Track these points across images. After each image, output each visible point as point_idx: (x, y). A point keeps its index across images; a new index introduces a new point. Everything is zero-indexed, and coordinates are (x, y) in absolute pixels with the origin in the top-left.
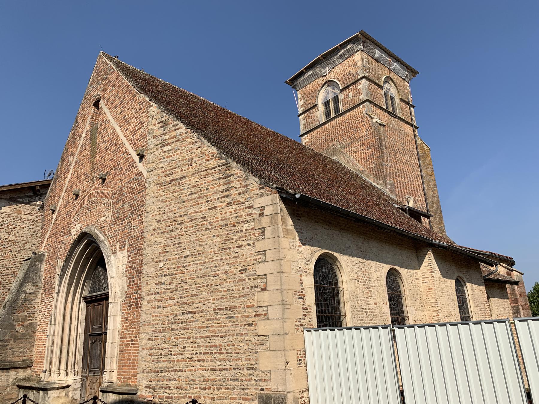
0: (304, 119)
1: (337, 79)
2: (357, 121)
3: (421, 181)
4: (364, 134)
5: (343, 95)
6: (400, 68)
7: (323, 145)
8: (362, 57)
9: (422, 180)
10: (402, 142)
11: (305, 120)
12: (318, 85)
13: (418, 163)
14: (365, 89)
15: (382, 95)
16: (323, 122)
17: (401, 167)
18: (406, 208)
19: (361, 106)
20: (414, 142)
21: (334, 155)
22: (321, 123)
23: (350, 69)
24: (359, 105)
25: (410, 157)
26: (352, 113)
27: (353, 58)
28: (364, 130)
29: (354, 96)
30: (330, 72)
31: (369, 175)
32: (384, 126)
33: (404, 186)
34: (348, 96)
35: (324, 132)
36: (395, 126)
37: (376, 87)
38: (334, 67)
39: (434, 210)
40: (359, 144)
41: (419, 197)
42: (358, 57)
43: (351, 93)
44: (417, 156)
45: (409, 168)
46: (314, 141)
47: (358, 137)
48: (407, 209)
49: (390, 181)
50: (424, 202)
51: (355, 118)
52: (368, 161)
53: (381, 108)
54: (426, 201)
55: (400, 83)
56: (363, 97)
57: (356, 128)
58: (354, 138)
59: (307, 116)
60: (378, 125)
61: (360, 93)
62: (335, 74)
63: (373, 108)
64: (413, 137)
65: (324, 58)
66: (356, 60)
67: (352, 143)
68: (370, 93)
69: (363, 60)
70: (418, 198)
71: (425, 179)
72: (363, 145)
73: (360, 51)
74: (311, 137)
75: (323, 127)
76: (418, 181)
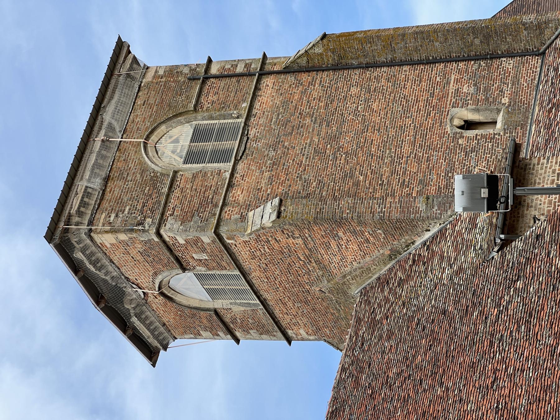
0: (249, 333)
1: (156, 274)
2: (267, 250)
3: (405, 68)
4: (300, 241)
5: (198, 268)
6: (113, 102)
7: (318, 306)
8: (107, 232)
9: (401, 64)
10: (308, 120)
11: (251, 331)
12: (165, 305)
13: (357, 72)
14: (188, 233)
15: (195, 176)
16: (258, 302)
17: (376, 137)
18: (501, 240)
19: (228, 241)
20: (305, 77)
21: (345, 293)
22: (262, 307)
23: (134, 252)
24: (227, 248)
25: (345, 98)
26: (243, 255)
27: (108, 246)
28: (291, 240)
29: (204, 250)
30: (137, 285)
31: (403, 240)
32: (281, 201)
33: (424, 136)
34: (201, 260)
35: (285, 304)
36: (271, 140)
37: (177, 193)
38: (126, 278)
39: (481, 42)
40: (323, 252)
41: (448, 83)
42: (107, 240)
43: (194, 255)
44: (341, 73)
45: (375, 107)
46: (305, 320)
47: (307, 251)
48: (502, 236)
49: (422, 206)
50: (461, 64)
51: (258, 253)
52: (367, 241)
53: (230, 185)
54: (457, 60)
55: (152, 101)
56: (207, 238)
57: (282, 253)
58: (307, 257)
59: (242, 327)
60: (281, 219)
61: (197, 241)
62: (143, 277)
63: (232, 213)
64: (291, 78)
65: (102, 297)
66: (114, 241)
67: (318, 262)
68: (196, 218)
69: (113, 231)
70: (452, 88)
71: (399, 55)
72: (328, 247)
73: (92, 234)
74: (297, 324)
75: (271, 303)
76: (407, 79)
